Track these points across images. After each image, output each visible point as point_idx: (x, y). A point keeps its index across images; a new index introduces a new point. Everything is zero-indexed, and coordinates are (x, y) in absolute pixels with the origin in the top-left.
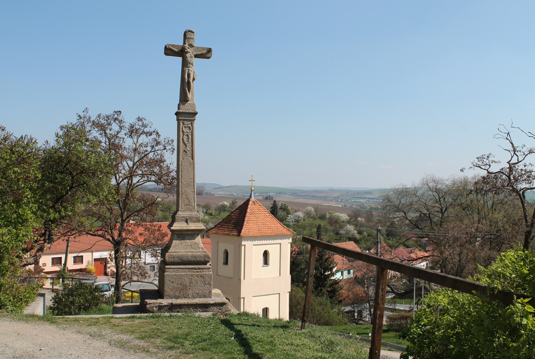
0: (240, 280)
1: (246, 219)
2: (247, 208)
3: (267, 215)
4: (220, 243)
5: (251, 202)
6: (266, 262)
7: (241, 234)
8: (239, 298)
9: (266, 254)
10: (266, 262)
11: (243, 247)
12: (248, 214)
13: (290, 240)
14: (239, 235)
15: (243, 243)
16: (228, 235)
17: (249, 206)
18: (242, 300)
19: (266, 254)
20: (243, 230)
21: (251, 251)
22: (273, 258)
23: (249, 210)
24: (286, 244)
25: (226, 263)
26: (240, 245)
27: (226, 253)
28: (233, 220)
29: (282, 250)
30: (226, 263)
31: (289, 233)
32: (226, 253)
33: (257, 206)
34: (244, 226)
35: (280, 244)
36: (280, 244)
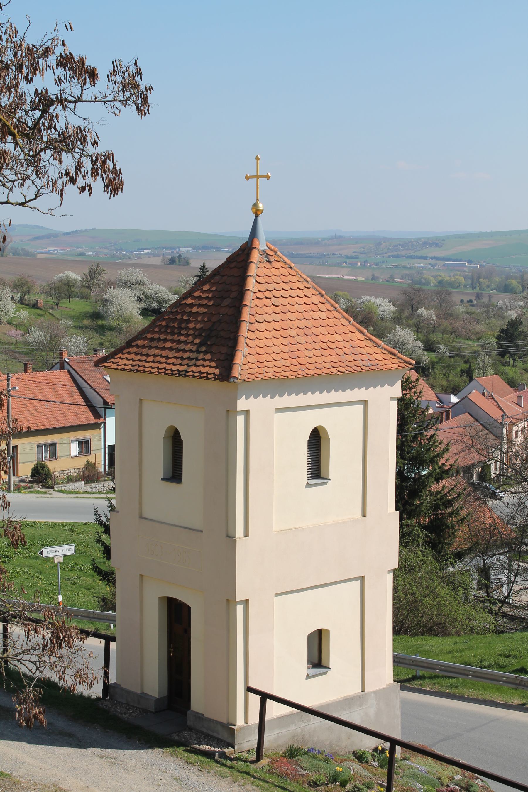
0: (231, 538)
1: (246, 315)
2: (243, 278)
3: (316, 299)
4: (146, 405)
5: (255, 256)
6: (317, 470)
7: (236, 372)
8: (230, 603)
9: (317, 440)
10: (317, 470)
11: (240, 419)
12: (249, 299)
13: (397, 390)
14: (225, 373)
15: (242, 404)
16: (182, 374)
17: (253, 270)
18: (240, 609)
19: (317, 440)
20: (239, 358)
21: (270, 430)
22: (340, 455)
23: (251, 284)
24: (384, 401)
25: (175, 474)
26: (231, 412)
27: (175, 440)
28: (203, 321)
29: (365, 425)
30: (175, 474)
31: (392, 363)
32: (175, 440)
33: (277, 271)
34: (242, 341)
35: (365, 403)
36: (365, 403)
